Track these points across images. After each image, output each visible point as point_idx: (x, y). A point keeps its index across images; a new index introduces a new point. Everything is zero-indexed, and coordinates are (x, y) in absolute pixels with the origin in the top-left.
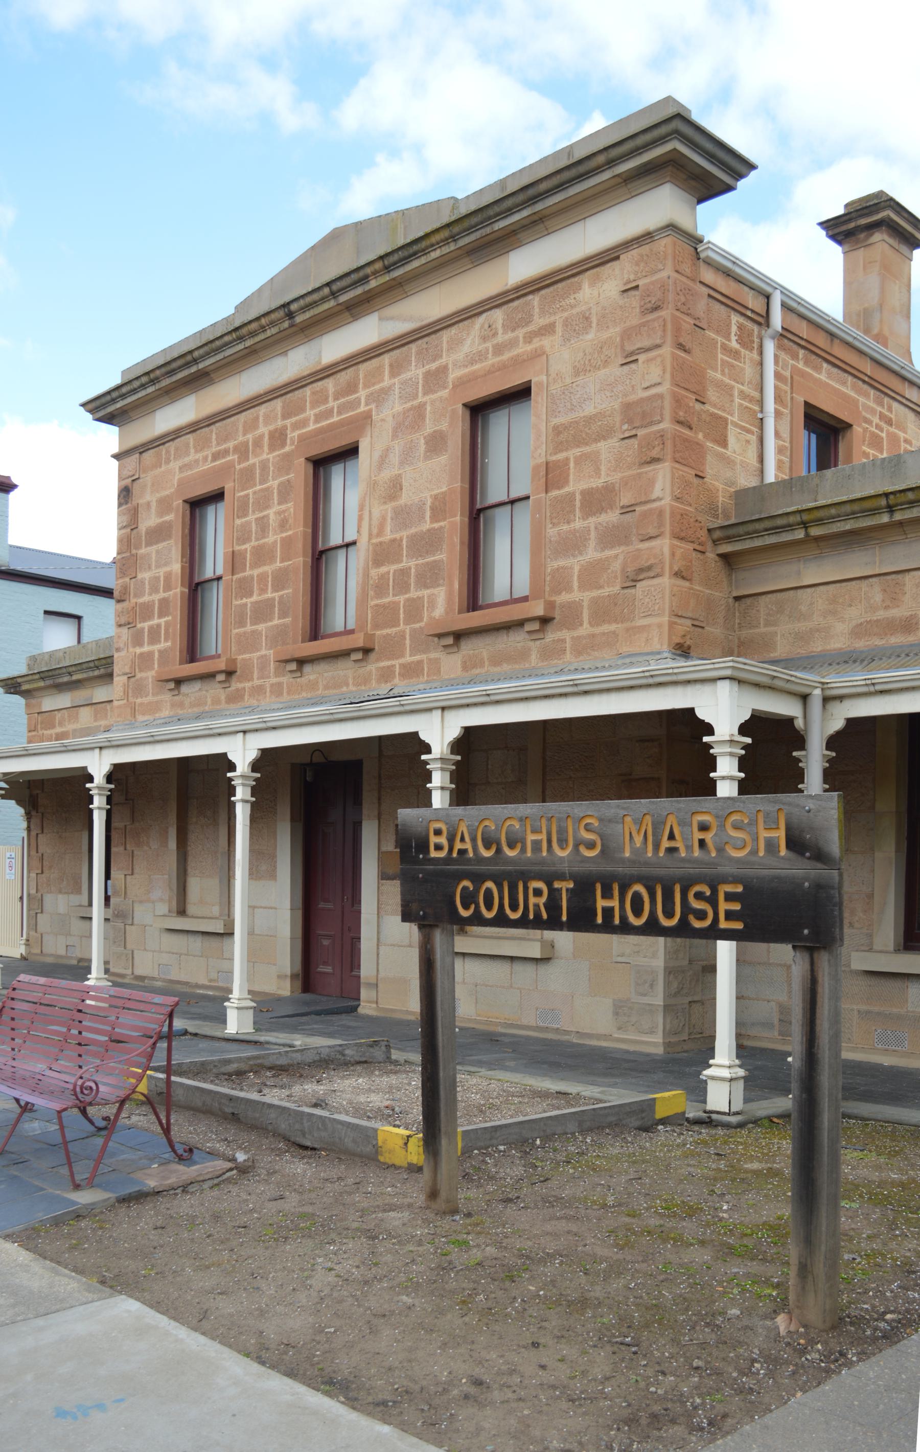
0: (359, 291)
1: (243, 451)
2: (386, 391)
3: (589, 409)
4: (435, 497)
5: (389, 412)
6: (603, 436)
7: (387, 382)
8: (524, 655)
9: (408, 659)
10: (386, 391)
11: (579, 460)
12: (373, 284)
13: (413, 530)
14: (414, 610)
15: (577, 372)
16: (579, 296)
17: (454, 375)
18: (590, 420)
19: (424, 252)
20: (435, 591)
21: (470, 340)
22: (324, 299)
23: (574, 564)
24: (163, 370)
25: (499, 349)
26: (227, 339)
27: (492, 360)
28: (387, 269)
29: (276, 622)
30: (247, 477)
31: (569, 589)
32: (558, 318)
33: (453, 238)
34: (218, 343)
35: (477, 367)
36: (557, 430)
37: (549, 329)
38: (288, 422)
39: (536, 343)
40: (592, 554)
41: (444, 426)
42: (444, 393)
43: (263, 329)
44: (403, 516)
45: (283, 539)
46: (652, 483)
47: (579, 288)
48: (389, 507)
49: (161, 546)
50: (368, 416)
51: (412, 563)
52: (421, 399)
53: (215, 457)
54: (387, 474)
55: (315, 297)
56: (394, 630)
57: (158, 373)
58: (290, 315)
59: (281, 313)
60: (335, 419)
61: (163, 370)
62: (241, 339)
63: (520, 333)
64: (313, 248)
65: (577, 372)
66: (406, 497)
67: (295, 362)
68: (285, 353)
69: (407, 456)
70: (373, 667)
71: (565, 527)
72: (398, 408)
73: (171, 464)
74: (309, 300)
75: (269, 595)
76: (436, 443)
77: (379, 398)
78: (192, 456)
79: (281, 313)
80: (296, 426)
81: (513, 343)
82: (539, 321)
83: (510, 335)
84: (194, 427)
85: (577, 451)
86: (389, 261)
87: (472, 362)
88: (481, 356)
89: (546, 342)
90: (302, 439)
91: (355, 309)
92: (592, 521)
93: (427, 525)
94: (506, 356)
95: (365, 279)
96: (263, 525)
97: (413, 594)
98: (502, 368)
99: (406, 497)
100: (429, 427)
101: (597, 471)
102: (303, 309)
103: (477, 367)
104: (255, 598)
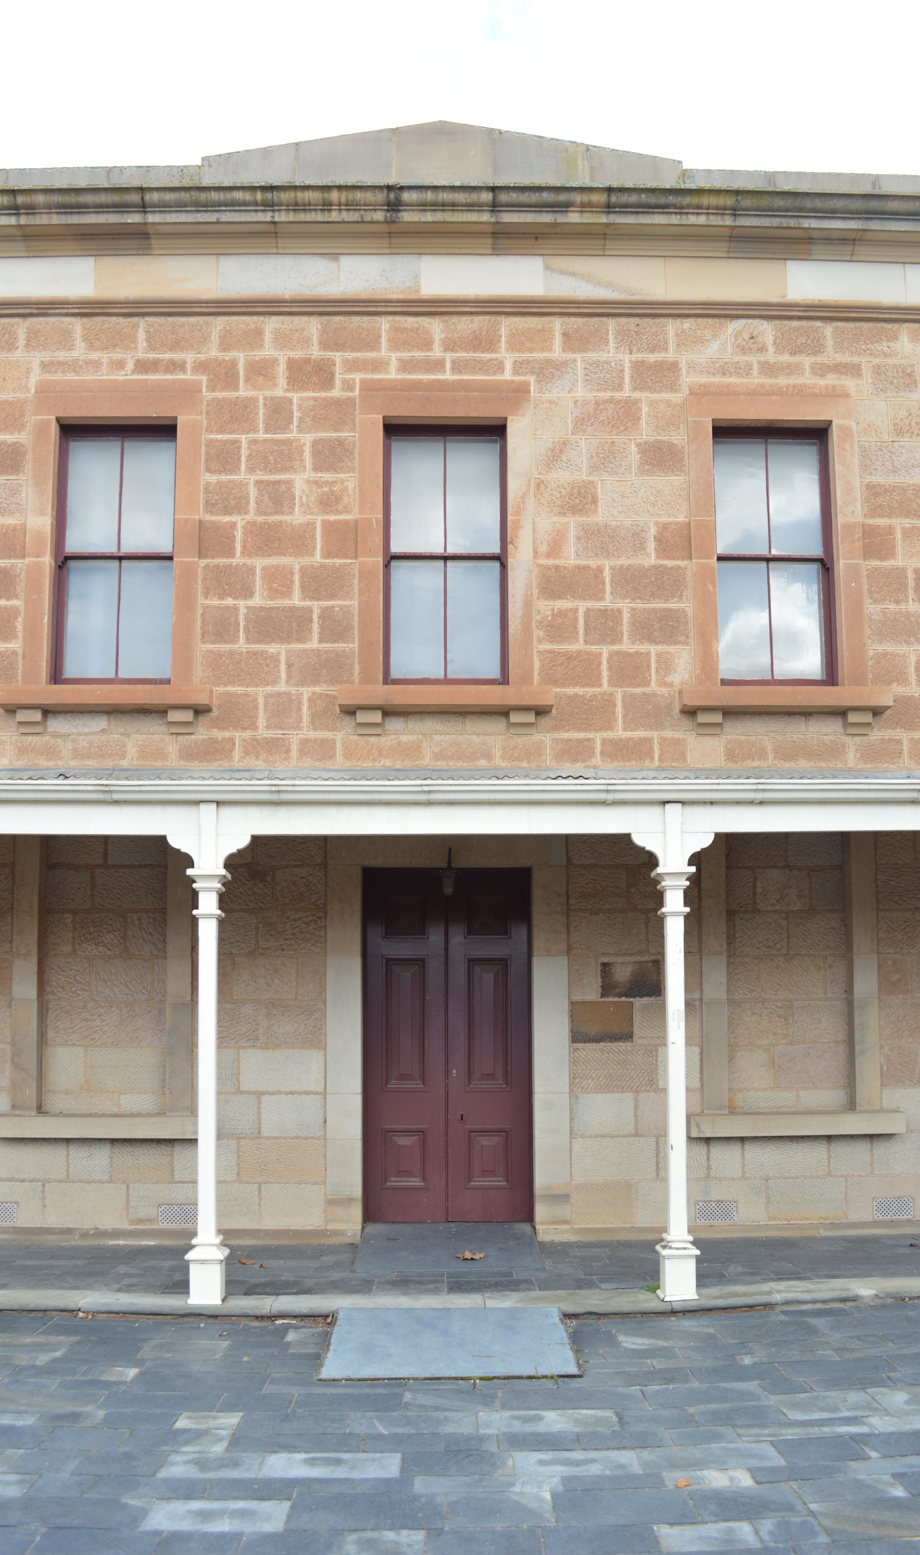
0: (546, 218)
1: (224, 375)
2: (560, 367)
4: (665, 527)
5: (571, 392)
7: (557, 352)
8: (836, 752)
9: (620, 732)
10: (560, 367)
12: (574, 217)
13: (623, 561)
14: (630, 670)
15: (899, 431)
16: (896, 346)
17: (687, 379)
19: (681, 210)
20: (672, 649)
21: (721, 343)
22: (471, 207)
24: (57, 199)
25: (768, 369)
26: (238, 195)
27: (756, 379)
28: (609, 208)
29: (314, 644)
30: (237, 415)
31: (901, 679)
32: (866, 363)
33: (735, 212)
34: (214, 196)
35: (732, 380)
36: (873, 491)
37: (854, 370)
38: (338, 357)
39: (831, 380)
41: (678, 437)
42: (676, 398)
43: (327, 206)
44: (600, 538)
45: (328, 527)
47: (896, 338)
48: (572, 523)
50: (522, 391)
51: (625, 606)
52: (627, 392)
53: (142, 366)
54: (562, 476)
55: (461, 197)
56: (590, 691)
57: (40, 199)
58: (394, 206)
59: (380, 197)
60: (448, 376)
61: (57, 199)
62: (269, 206)
63: (807, 361)
64: (395, 131)
65: (899, 431)
66: (601, 515)
67: (359, 274)
68: (335, 256)
69: (605, 459)
70: (545, 738)
71: (892, 607)
72: (581, 392)
73: (19, 354)
74: (439, 197)
75: (296, 600)
76: (660, 457)
77: (548, 371)
78: (79, 351)
79: (380, 197)
80: (352, 366)
81: (792, 369)
82: (831, 355)
83: (785, 358)
84: (88, 309)
85: (907, 522)
86: (616, 199)
88: (744, 370)
89: (849, 384)
90: (367, 386)
91: (503, 241)
94: (783, 381)
95: (566, 207)
96: (278, 496)
97: (626, 645)
98: (780, 392)
99: (601, 515)
100: (646, 432)
102: (423, 206)
103: (732, 380)
104: (257, 601)
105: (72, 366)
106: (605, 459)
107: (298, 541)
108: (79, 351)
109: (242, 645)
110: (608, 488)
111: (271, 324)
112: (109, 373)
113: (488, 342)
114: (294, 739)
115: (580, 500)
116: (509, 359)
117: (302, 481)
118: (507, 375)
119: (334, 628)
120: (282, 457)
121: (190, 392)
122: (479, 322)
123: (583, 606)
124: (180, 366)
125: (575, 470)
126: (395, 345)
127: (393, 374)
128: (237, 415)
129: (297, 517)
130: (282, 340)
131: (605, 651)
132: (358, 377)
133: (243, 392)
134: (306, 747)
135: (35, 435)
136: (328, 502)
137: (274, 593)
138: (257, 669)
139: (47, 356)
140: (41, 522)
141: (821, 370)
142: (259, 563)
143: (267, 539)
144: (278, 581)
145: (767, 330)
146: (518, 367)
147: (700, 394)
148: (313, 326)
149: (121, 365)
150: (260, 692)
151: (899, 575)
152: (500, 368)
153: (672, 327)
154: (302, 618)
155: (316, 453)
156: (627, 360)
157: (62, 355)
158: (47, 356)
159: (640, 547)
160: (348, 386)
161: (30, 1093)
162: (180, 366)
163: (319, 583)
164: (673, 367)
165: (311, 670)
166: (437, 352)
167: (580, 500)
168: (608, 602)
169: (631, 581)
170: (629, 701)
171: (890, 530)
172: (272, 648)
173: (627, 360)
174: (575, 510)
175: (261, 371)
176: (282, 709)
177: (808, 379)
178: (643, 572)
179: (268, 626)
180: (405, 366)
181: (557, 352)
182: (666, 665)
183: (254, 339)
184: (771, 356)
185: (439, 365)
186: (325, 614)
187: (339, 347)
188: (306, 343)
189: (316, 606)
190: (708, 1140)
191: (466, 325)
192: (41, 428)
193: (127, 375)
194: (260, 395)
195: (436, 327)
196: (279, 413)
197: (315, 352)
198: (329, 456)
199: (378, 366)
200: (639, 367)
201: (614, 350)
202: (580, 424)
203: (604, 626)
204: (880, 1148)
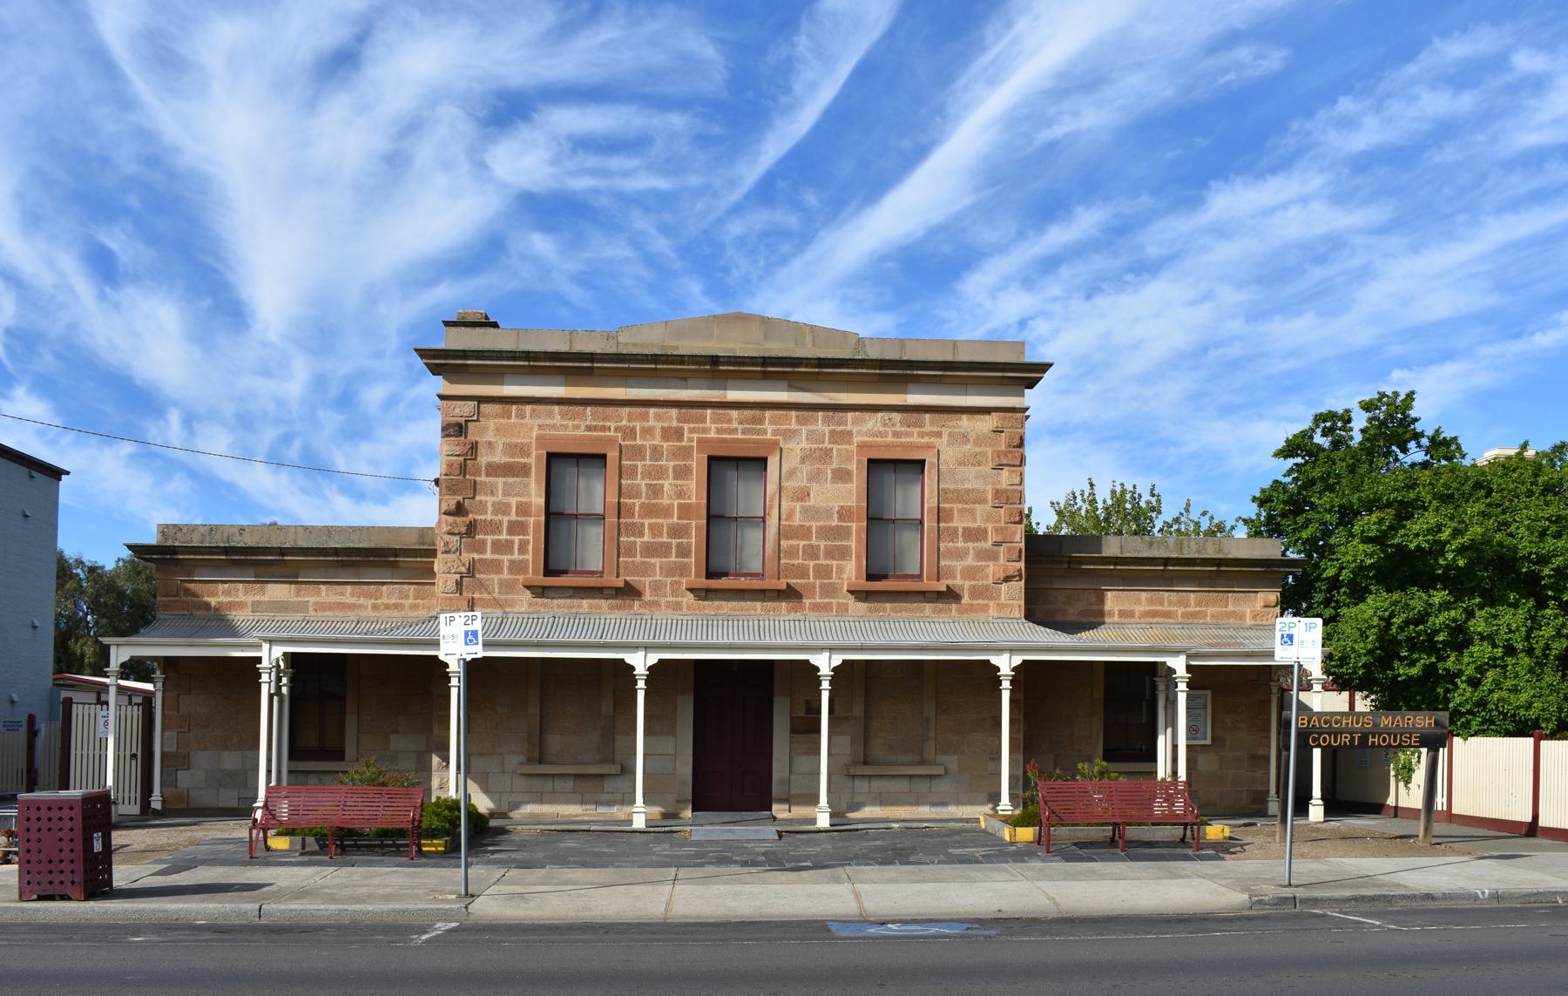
1: (630, 433)
3: (968, 486)
6: (983, 501)
7: (794, 426)
10: (795, 432)
11: (960, 511)
14: (823, 572)
17: (856, 440)
18: (968, 491)
21: (874, 422)
23: (959, 565)
25: (897, 434)
27: (890, 439)
30: (638, 452)
37: (939, 435)
38: (686, 426)
39: (926, 440)
40: (970, 561)
46: (1014, 533)
48: (798, 505)
49: (510, 480)
51: (822, 544)
52: (827, 445)
53: (589, 428)
63: (915, 430)
66: (811, 502)
69: (815, 477)
72: (804, 444)
73: (527, 420)
76: (842, 475)
77: (789, 434)
80: (692, 431)
82: (928, 428)
87: (874, 435)
88: (880, 434)
92: (971, 545)
93: (835, 523)
94: (903, 440)
96: (656, 491)
97: (823, 562)
98: (902, 445)
99: (811, 502)
101: (975, 519)
104: (646, 539)
105: (554, 427)
106: (815, 477)
107: (667, 512)
108: (557, 420)
109: (638, 559)
110: (815, 489)
111: (652, 411)
112: (572, 430)
113: (761, 421)
114: (663, 600)
115: (803, 495)
116: (770, 428)
117: (667, 484)
118: (769, 436)
119: (683, 551)
120: (660, 473)
121: (612, 440)
122: (757, 412)
123: (802, 543)
124: (604, 429)
125: (800, 481)
126: (714, 421)
127: (713, 435)
128: (638, 452)
129: (666, 501)
130: (658, 418)
131: (812, 563)
132: (695, 436)
133: (639, 442)
134: (668, 605)
135: (535, 460)
136: (680, 494)
137: (654, 535)
138: (646, 570)
139: (540, 422)
140: (538, 500)
141: (922, 435)
142: (647, 522)
143: (649, 511)
144: (656, 530)
145: (896, 416)
146: (775, 432)
147: (861, 446)
148: (674, 412)
149: (578, 427)
150: (647, 580)
151: (955, 530)
152: (765, 432)
153: (850, 415)
154: (669, 546)
155: (675, 471)
156: (827, 429)
157: (548, 422)
158: (540, 422)
159: (830, 517)
160: (691, 440)
161: (536, 754)
162: (604, 429)
163: (676, 531)
164: (850, 433)
165: (672, 570)
166: (735, 425)
167: (803, 495)
168: (814, 541)
169: (824, 532)
170: (822, 586)
171: (951, 510)
172: (653, 560)
173: (827, 429)
174: (799, 499)
175: (647, 432)
176: (657, 588)
177: (915, 439)
178: (831, 528)
179: (650, 550)
180: (719, 431)
181: (794, 426)
182: (840, 570)
183: (645, 417)
184: (898, 428)
185: (735, 431)
186: (678, 545)
187: (687, 421)
188: (670, 419)
189: (674, 542)
190: (853, 777)
191: (748, 413)
192: (538, 457)
193: (581, 432)
194: (647, 443)
195: (734, 414)
196: (656, 452)
197: (675, 424)
198: (682, 473)
199: (705, 430)
200: (833, 432)
201: (820, 422)
202: (803, 461)
203: (812, 552)
204: (935, 782)
